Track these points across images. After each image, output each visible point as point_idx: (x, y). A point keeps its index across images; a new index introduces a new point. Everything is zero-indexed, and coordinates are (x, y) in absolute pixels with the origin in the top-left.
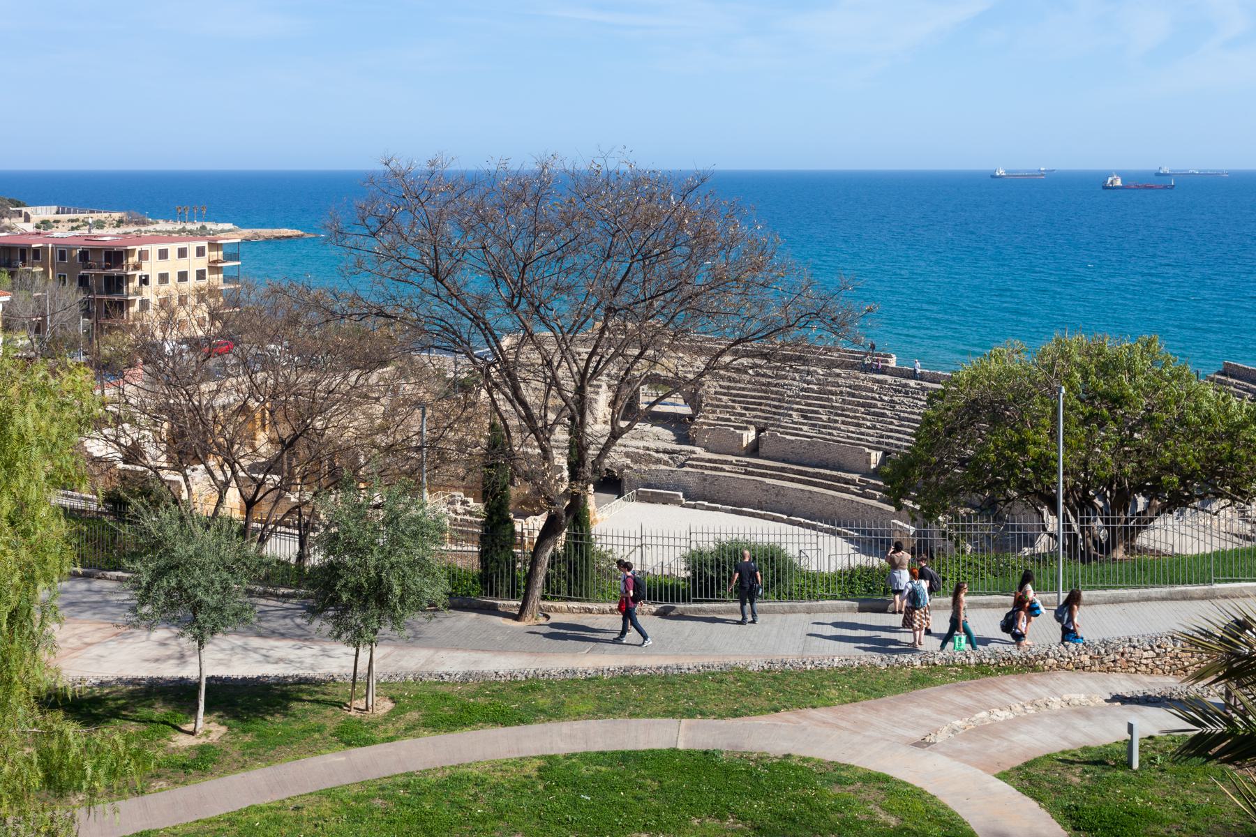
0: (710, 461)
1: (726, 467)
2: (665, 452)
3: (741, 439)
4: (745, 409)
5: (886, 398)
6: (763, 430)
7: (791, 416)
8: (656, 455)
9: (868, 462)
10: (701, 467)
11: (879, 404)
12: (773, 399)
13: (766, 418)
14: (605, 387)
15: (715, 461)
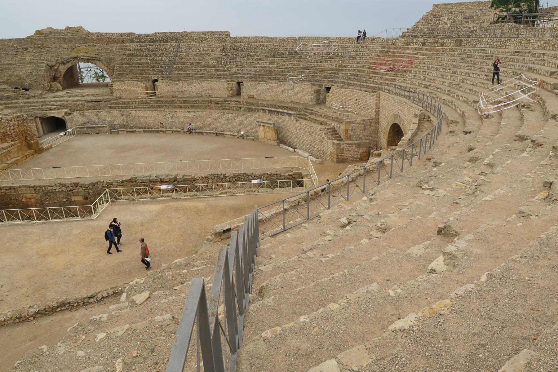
6: (156, 81)
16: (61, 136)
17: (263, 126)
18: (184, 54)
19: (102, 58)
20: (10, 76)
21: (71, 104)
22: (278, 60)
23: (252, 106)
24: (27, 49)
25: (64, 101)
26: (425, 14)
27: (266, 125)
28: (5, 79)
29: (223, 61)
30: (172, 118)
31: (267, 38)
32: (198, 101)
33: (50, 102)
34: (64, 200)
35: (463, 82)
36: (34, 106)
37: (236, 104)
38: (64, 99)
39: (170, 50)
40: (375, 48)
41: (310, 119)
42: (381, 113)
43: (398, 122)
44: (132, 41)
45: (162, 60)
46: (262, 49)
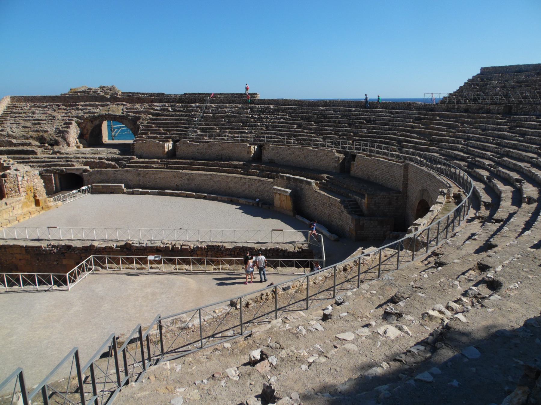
0: (143, 163)
1: (154, 166)
2: (113, 160)
3: (164, 147)
4: (167, 130)
5: (256, 116)
6: (178, 141)
7: (196, 132)
8: (107, 162)
9: (249, 152)
10: (137, 167)
11: (252, 120)
12: (184, 124)
13: (181, 134)
14: (74, 122)
15: (147, 163)
16: (74, 193)
17: (280, 194)
18: (211, 115)
20: (37, 131)
21: (91, 161)
24: (58, 106)
25: (85, 158)
27: (283, 193)
30: (188, 180)
33: (71, 158)
34: (55, 263)
36: (54, 162)
38: (86, 156)
42: (409, 187)
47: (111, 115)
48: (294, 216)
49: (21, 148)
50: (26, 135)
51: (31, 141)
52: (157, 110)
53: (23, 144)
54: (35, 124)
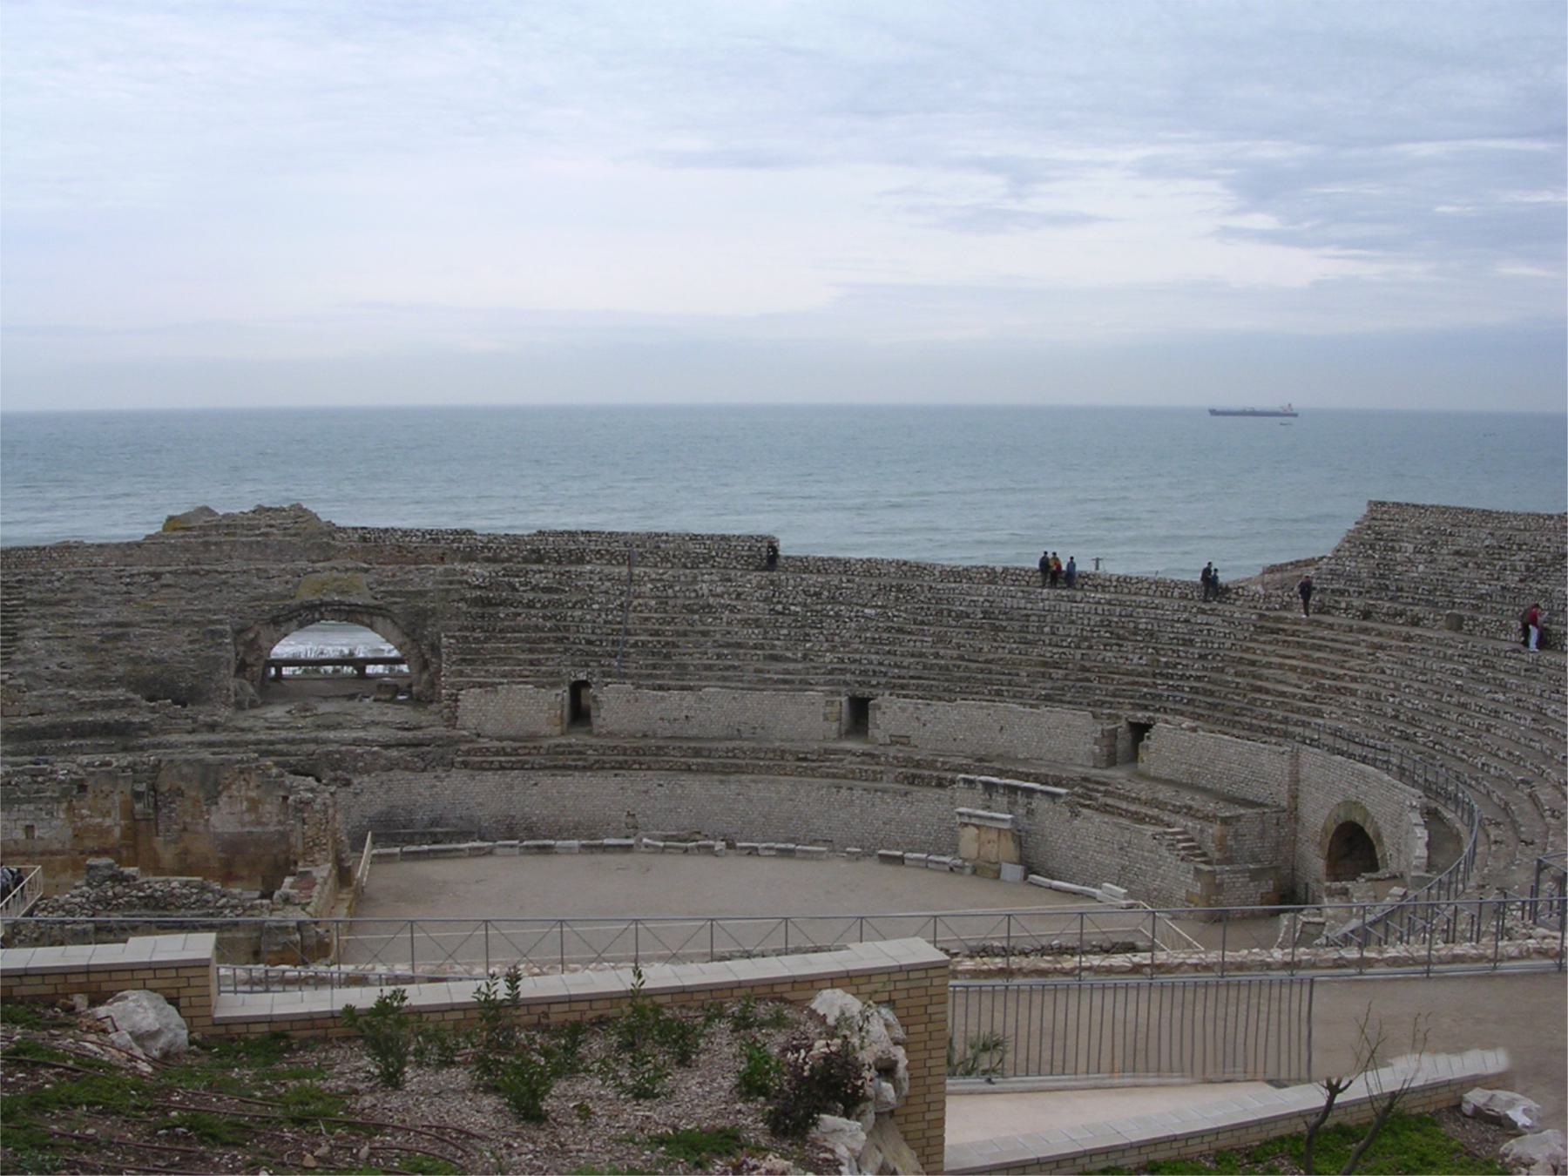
4: (531, 651)
19: (396, 609)
20: (135, 661)
21: (339, 752)
22: (957, 636)
23: (922, 773)
24: (157, 576)
25: (316, 741)
26: (1352, 526)
27: (988, 823)
28: (120, 669)
29: (785, 632)
31: (905, 563)
32: (741, 749)
35: (1488, 731)
37: (863, 763)
39: (603, 588)
40: (1237, 615)
41: (1105, 809)
43: (1358, 819)
44: (469, 557)
45: (581, 620)
46: (897, 598)
47: (341, 603)
48: (1026, 878)
49: (102, 716)
50: (102, 673)
51: (120, 693)
52: (479, 587)
53: (109, 705)
54: (117, 637)
